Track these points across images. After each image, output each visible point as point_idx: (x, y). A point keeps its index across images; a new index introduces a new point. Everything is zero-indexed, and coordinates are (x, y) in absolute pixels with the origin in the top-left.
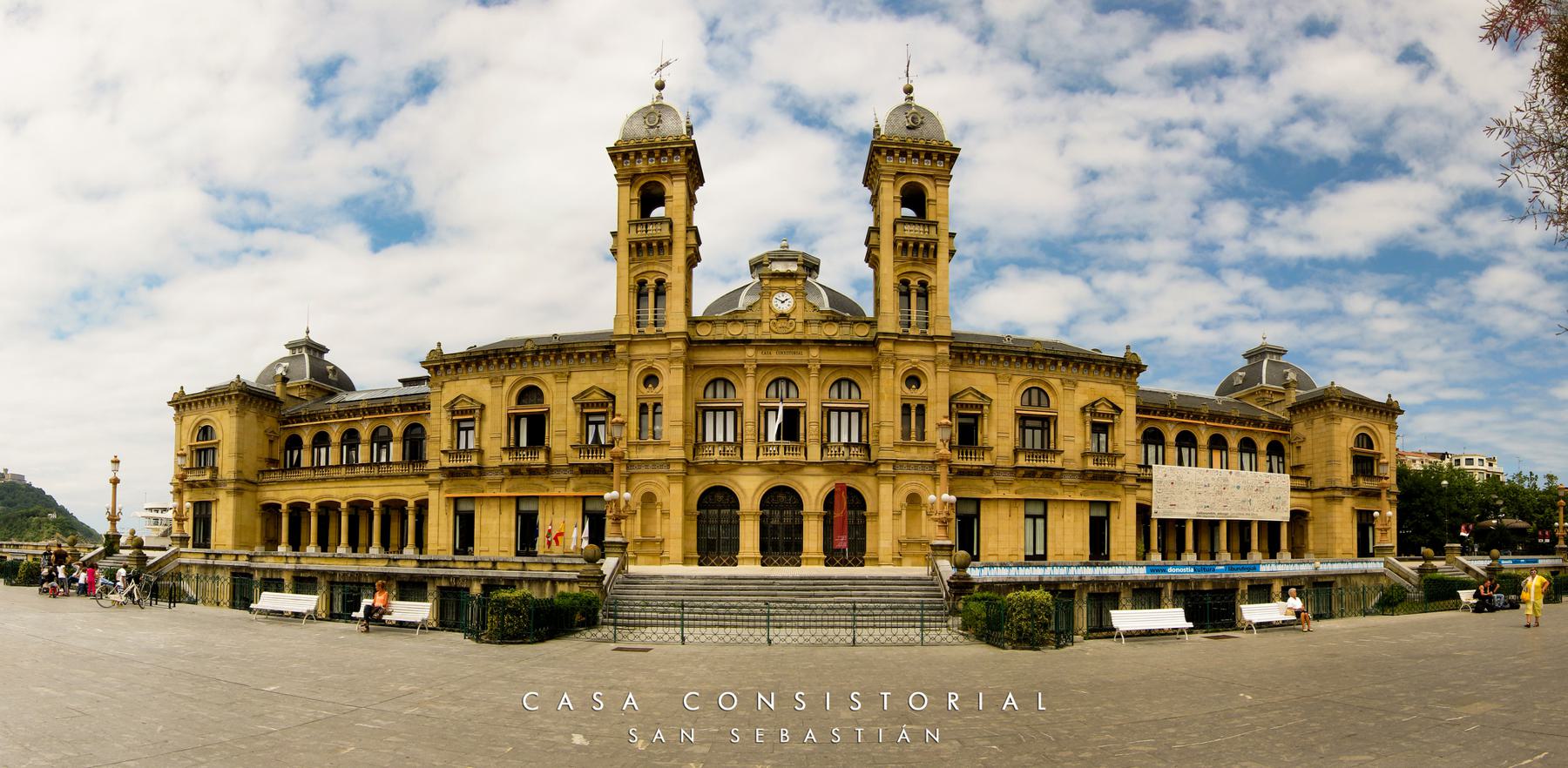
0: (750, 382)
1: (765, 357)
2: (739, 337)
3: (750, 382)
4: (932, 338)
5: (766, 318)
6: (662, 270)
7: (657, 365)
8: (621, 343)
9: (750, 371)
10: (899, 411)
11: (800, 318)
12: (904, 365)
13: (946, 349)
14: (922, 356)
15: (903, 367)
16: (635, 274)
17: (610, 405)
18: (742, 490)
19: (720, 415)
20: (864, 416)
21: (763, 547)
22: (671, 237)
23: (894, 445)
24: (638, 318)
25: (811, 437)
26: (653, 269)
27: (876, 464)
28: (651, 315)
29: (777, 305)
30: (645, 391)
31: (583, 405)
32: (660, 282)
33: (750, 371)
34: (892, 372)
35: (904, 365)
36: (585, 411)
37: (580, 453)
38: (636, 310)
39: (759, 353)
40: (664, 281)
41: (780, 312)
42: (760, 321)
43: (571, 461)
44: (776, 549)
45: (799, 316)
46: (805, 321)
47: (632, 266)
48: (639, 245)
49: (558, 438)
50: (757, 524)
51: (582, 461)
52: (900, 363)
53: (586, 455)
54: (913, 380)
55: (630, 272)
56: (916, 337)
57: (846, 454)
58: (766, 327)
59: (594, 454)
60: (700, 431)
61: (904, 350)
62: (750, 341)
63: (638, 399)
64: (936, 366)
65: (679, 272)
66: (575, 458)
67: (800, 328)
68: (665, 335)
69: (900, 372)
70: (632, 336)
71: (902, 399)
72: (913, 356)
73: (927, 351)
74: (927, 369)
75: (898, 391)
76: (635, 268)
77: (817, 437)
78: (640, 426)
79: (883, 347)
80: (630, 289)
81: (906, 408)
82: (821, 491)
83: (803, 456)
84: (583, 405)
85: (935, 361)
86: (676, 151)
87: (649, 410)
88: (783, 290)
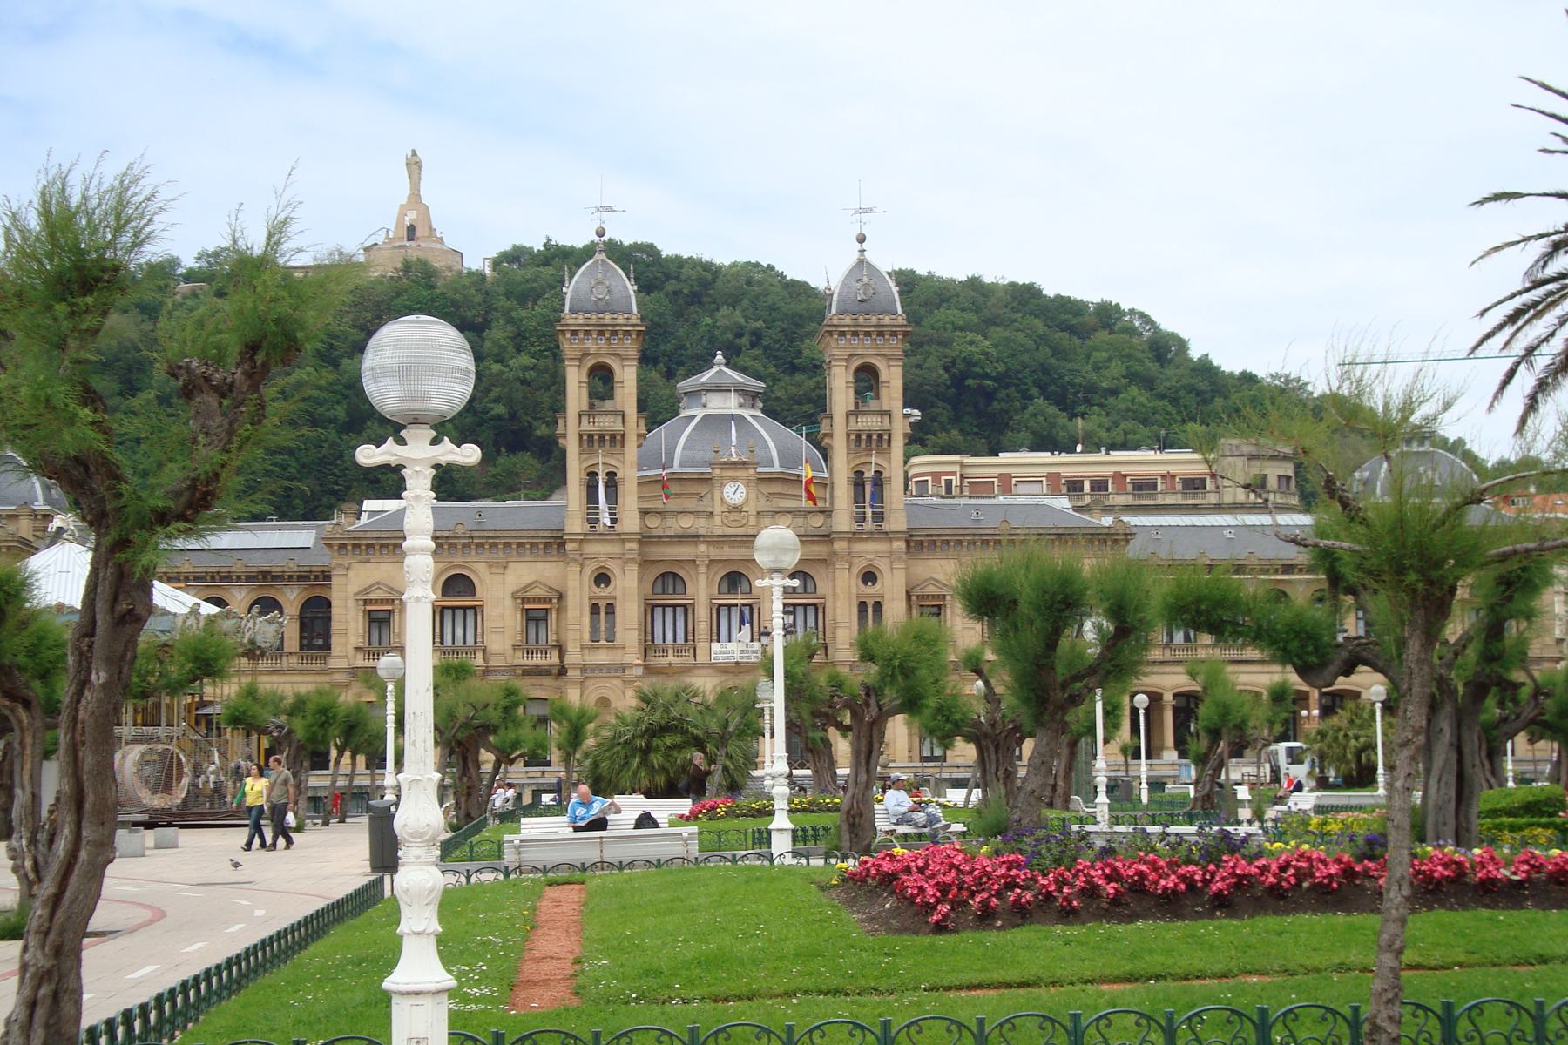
0: (702, 579)
1: (718, 552)
2: (692, 531)
3: (702, 579)
5: (718, 509)
6: (613, 462)
7: (610, 564)
8: (572, 541)
9: (702, 568)
10: (855, 610)
13: (903, 545)
15: (859, 565)
16: (585, 465)
17: (555, 601)
19: (669, 611)
20: (820, 611)
26: (602, 461)
33: (702, 568)
36: (527, 606)
45: (751, 508)
52: (856, 560)
54: (869, 577)
56: (871, 533)
58: (718, 520)
60: (649, 629)
61: (858, 547)
64: (892, 563)
67: (752, 521)
68: (619, 534)
69: (855, 570)
72: (868, 553)
73: (882, 547)
74: (883, 565)
75: (854, 590)
76: (586, 459)
79: (837, 545)
81: (862, 606)
87: (602, 612)
88: (734, 480)
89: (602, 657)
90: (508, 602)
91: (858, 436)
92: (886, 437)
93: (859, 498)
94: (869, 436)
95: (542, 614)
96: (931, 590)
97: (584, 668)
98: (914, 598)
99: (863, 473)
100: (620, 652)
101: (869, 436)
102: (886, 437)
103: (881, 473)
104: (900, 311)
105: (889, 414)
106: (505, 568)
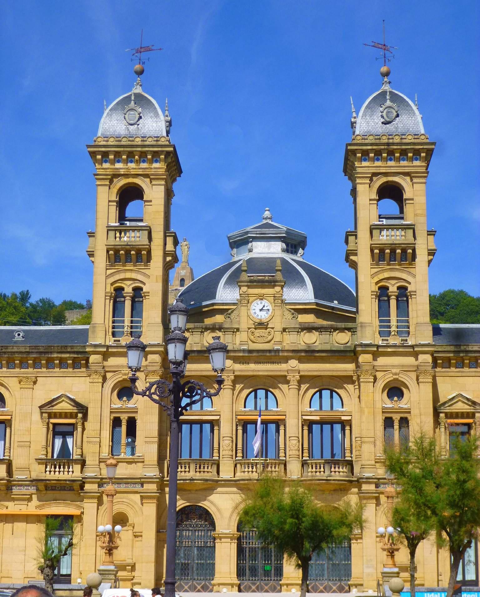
4: (413, 347)
6: (139, 277)
9: (228, 383)
11: (279, 327)
12: (385, 375)
13: (429, 358)
14: (403, 366)
15: (383, 379)
16: (112, 279)
17: (80, 415)
18: (218, 510)
21: (240, 573)
22: (150, 246)
23: (376, 462)
24: (113, 327)
25: (291, 453)
27: (358, 483)
28: (127, 323)
29: (255, 313)
30: (118, 404)
31: (51, 415)
32: (137, 290)
34: (372, 384)
35: (385, 375)
37: (46, 467)
38: (111, 319)
39: (238, 367)
40: (141, 289)
41: (258, 321)
42: (238, 330)
43: (34, 476)
44: (254, 572)
45: (277, 324)
46: (284, 330)
47: (109, 272)
48: (117, 251)
49: (20, 450)
50: (234, 546)
51: (48, 476)
53: (53, 469)
55: (107, 277)
57: (327, 473)
59: (62, 469)
61: (382, 361)
63: (111, 412)
65: (157, 281)
66: (38, 472)
69: (380, 384)
70: (108, 347)
71: (383, 412)
72: (393, 366)
73: (410, 360)
74: (409, 379)
75: (379, 406)
76: (112, 275)
77: (297, 453)
78: (112, 441)
79: (362, 358)
80: (106, 296)
83: (283, 474)
84: (50, 416)
85: (418, 371)
86: (156, 154)
88: (261, 297)
89: (123, 471)
90: (36, 415)
91: (382, 251)
92: (410, 251)
93: (383, 311)
94: (393, 251)
95: (70, 429)
96: (461, 407)
97: (101, 483)
98: (442, 415)
99: (387, 288)
100: (140, 465)
101: (393, 251)
102: (410, 251)
103: (406, 288)
104: (423, 132)
105: (411, 227)
106: (35, 383)
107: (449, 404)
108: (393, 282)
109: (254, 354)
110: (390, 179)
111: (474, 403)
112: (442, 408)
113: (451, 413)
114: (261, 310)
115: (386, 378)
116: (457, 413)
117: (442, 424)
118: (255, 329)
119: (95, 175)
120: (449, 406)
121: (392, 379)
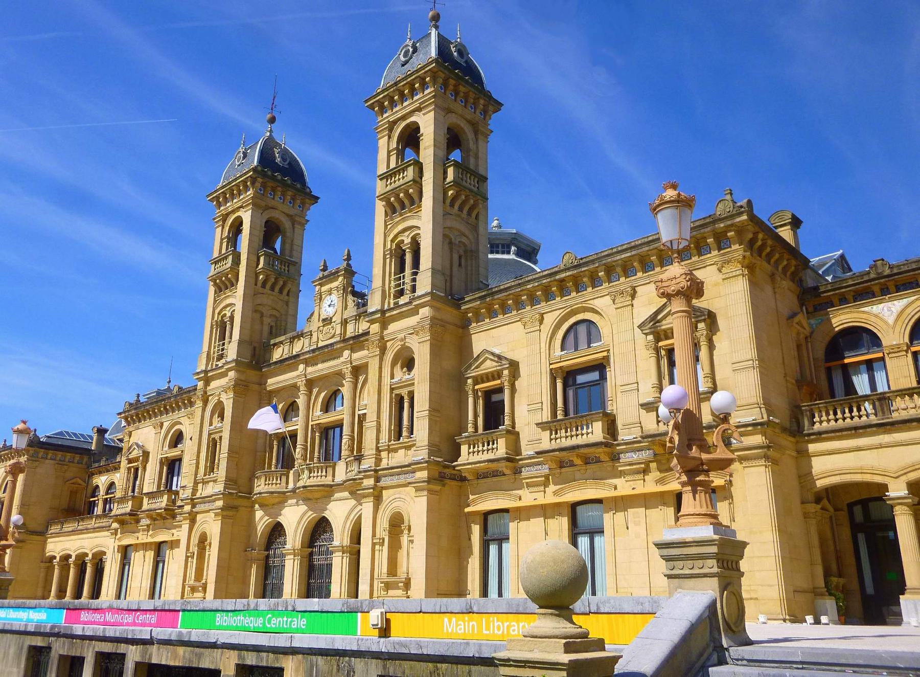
15: (392, 349)
62: (297, 356)
69: (389, 356)
82: (347, 518)
88: (330, 292)
107: (476, 365)
108: (407, 233)
109: (317, 353)
110: (408, 121)
111: (500, 357)
112: (469, 372)
113: (481, 376)
114: (329, 306)
115: (395, 346)
116: (487, 374)
117: (470, 392)
118: (324, 326)
119: (214, 219)
120: (477, 367)
121: (400, 347)
